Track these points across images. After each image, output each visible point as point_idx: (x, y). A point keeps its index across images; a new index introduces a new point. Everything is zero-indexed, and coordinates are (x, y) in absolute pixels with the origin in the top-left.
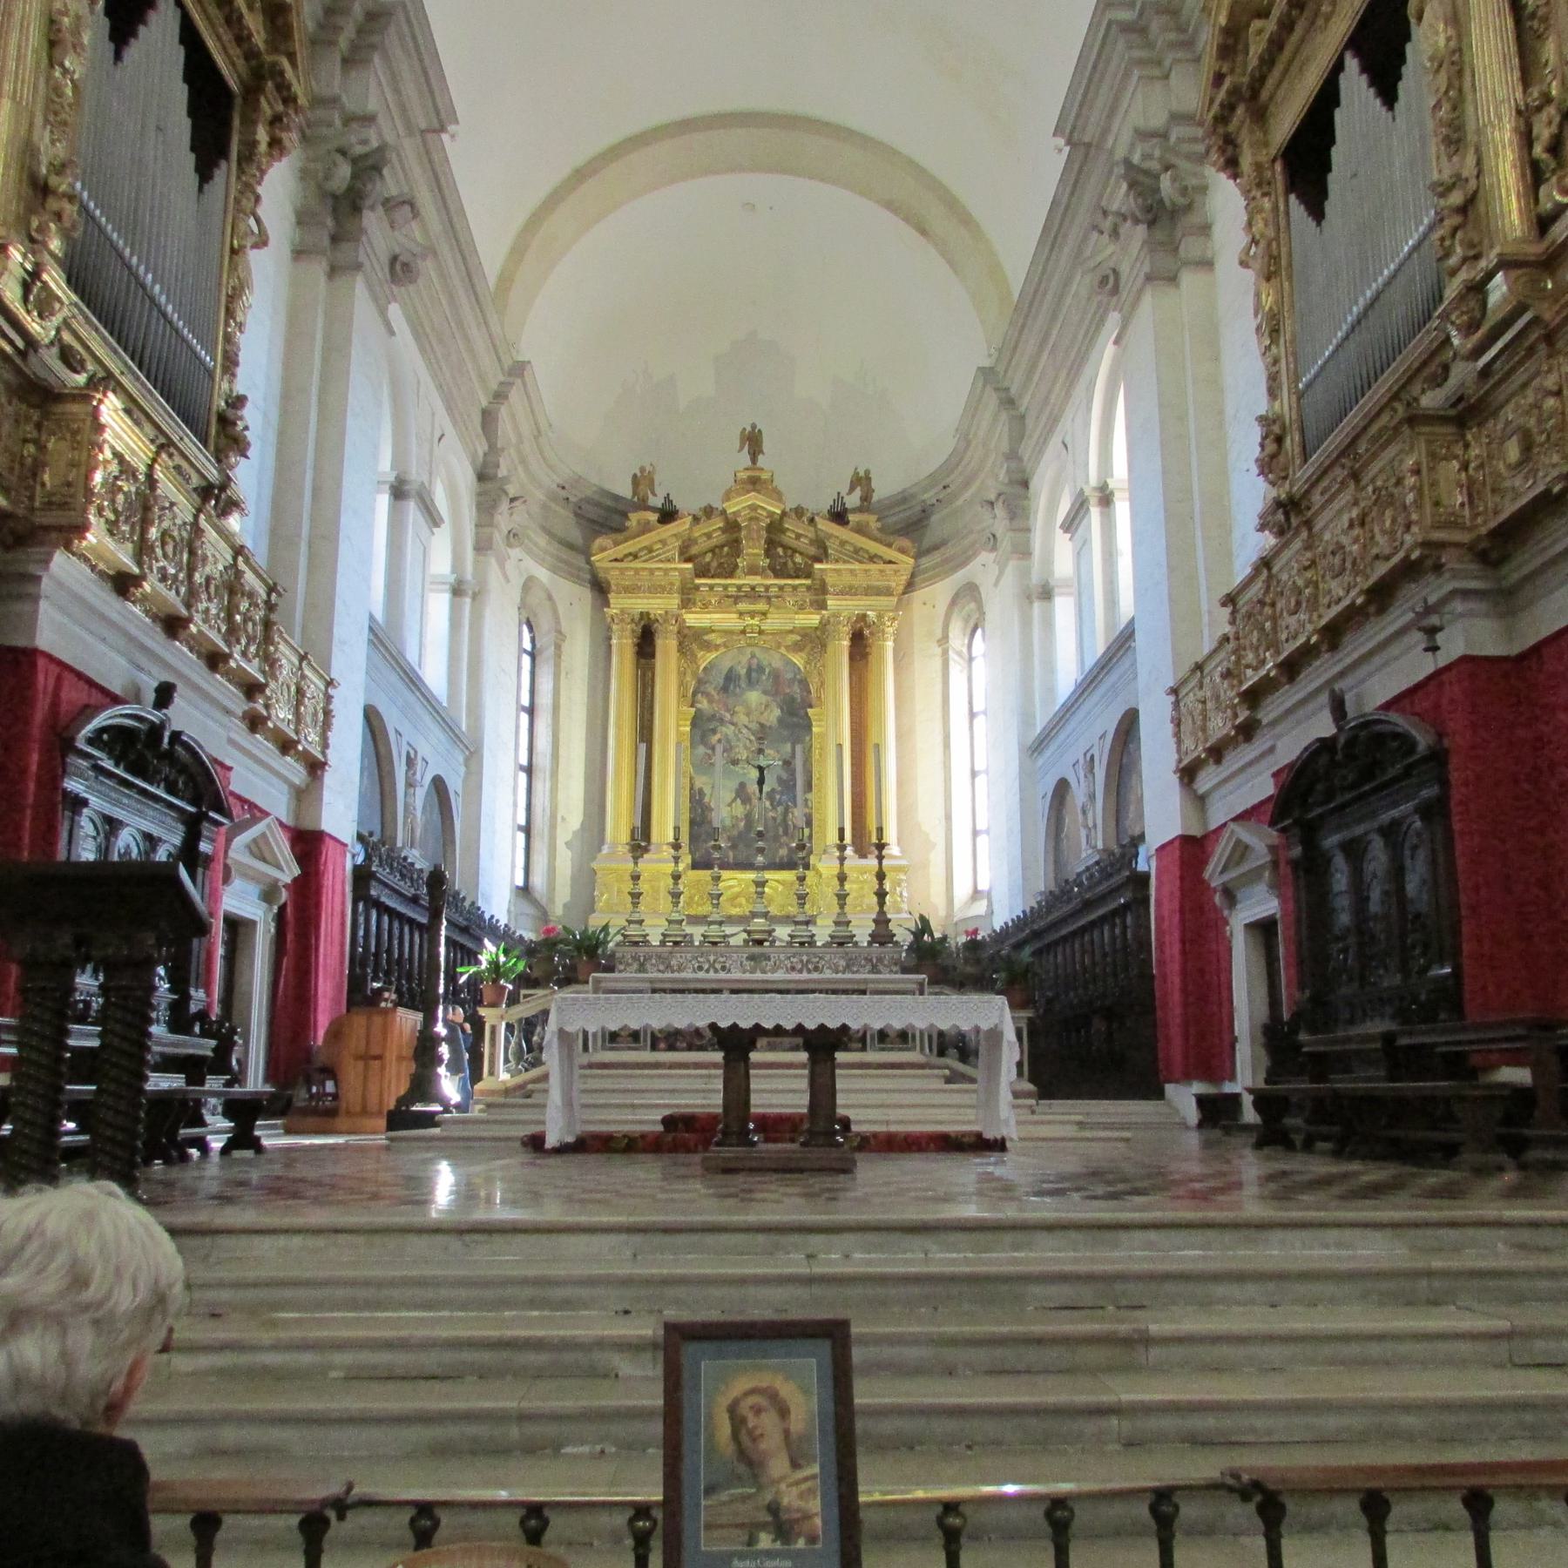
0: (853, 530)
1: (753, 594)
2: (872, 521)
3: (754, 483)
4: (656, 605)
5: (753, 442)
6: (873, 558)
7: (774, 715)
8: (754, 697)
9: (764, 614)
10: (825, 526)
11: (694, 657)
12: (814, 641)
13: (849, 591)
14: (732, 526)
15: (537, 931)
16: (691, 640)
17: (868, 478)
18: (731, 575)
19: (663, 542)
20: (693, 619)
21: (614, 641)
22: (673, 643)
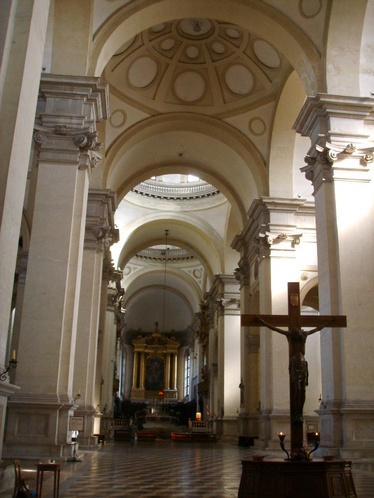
0: (172, 340)
1: (156, 348)
2: (174, 338)
3: (157, 332)
4: (141, 350)
5: (157, 324)
6: (174, 344)
7: (158, 366)
8: (156, 363)
9: (157, 351)
10: (167, 339)
11: (147, 358)
12: (165, 355)
13: (170, 348)
14: (153, 337)
15: (123, 399)
16: (146, 354)
17: (174, 330)
18: (153, 344)
19: (143, 341)
20: (147, 351)
21: (135, 356)
22: (144, 357)
